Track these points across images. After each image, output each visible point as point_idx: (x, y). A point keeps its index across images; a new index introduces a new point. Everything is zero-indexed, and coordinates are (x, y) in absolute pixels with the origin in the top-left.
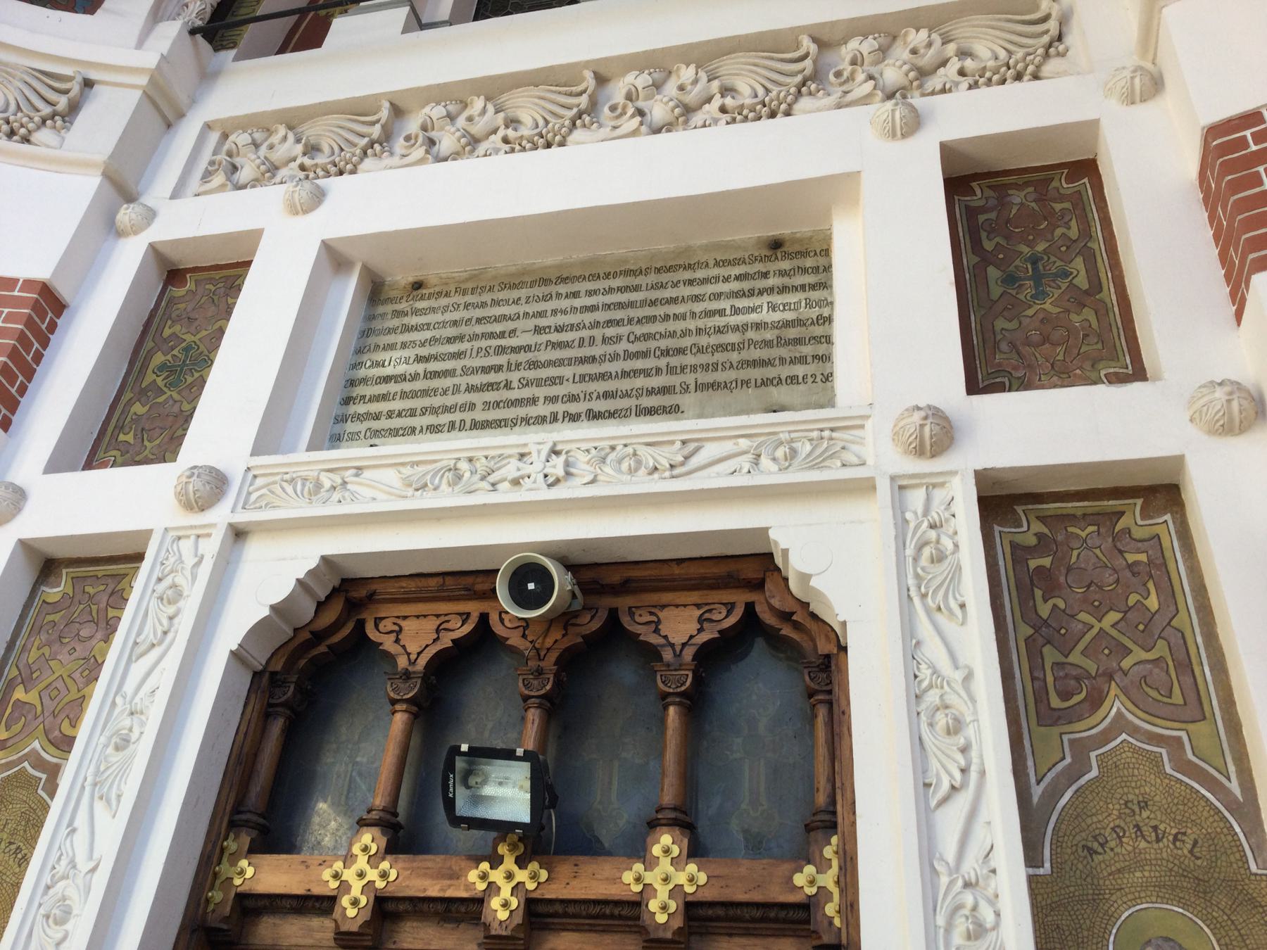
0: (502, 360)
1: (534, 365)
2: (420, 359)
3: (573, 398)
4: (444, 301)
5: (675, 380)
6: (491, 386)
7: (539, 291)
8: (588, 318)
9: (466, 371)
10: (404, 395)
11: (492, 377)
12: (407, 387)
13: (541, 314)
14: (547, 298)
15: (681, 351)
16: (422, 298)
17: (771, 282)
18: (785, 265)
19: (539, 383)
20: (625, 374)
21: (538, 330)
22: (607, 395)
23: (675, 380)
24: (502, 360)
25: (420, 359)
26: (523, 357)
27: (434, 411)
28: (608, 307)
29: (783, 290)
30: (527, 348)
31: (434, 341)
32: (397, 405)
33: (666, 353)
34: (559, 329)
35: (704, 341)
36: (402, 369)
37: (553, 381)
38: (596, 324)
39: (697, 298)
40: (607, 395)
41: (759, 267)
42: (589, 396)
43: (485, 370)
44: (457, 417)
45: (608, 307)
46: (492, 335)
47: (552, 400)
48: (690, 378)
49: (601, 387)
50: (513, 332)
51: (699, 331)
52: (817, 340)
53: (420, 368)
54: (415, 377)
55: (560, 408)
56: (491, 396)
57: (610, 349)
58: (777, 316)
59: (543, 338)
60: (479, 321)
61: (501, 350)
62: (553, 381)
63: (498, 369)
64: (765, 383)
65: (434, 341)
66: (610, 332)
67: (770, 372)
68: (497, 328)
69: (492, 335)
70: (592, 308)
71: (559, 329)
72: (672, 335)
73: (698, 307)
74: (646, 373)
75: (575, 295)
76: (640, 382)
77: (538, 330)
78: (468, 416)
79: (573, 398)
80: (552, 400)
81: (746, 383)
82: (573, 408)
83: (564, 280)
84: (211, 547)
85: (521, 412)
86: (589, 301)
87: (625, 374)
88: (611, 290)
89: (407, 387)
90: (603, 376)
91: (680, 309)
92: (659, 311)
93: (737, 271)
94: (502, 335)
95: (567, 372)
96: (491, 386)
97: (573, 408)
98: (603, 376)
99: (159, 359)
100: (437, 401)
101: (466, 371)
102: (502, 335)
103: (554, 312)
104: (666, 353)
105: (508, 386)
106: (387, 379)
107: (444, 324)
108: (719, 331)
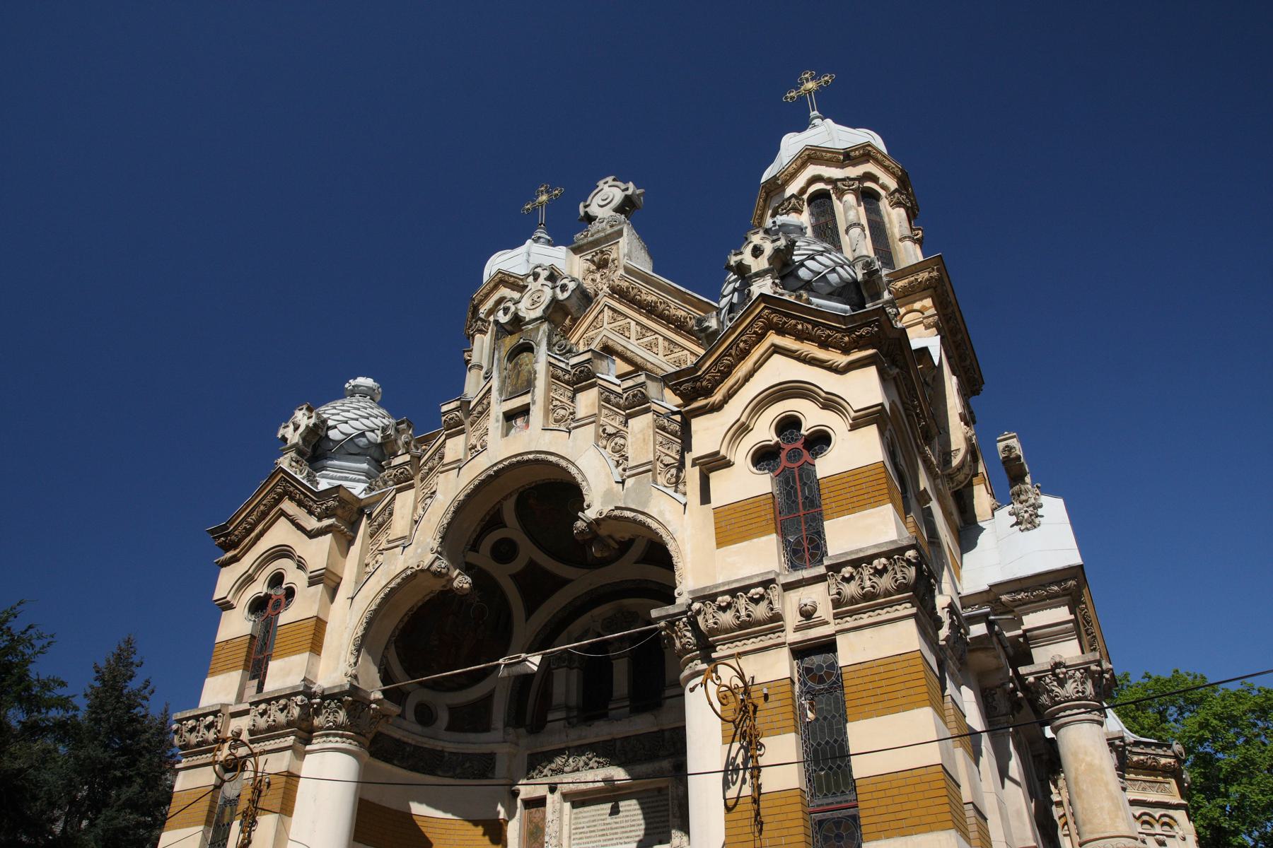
0: (605, 827)
1: (612, 829)
3: (621, 838)
6: (603, 835)
9: (598, 831)
11: (604, 832)
19: (613, 834)
20: (631, 831)
22: (628, 837)
24: (605, 827)
26: (609, 826)
30: (609, 824)
31: (589, 821)
32: (585, 840)
37: (616, 833)
40: (628, 837)
47: (616, 839)
55: (618, 841)
56: (604, 838)
57: (627, 824)
61: (604, 824)
62: (616, 833)
63: (604, 830)
66: (627, 819)
69: (602, 820)
78: (600, 843)
79: (621, 838)
80: (616, 839)
81: (654, 833)
82: (621, 841)
90: (626, 832)
96: (603, 835)
97: (621, 841)
98: (626, 832)
100: (593, 839)
101: (598, 831)
107: (591, 816)
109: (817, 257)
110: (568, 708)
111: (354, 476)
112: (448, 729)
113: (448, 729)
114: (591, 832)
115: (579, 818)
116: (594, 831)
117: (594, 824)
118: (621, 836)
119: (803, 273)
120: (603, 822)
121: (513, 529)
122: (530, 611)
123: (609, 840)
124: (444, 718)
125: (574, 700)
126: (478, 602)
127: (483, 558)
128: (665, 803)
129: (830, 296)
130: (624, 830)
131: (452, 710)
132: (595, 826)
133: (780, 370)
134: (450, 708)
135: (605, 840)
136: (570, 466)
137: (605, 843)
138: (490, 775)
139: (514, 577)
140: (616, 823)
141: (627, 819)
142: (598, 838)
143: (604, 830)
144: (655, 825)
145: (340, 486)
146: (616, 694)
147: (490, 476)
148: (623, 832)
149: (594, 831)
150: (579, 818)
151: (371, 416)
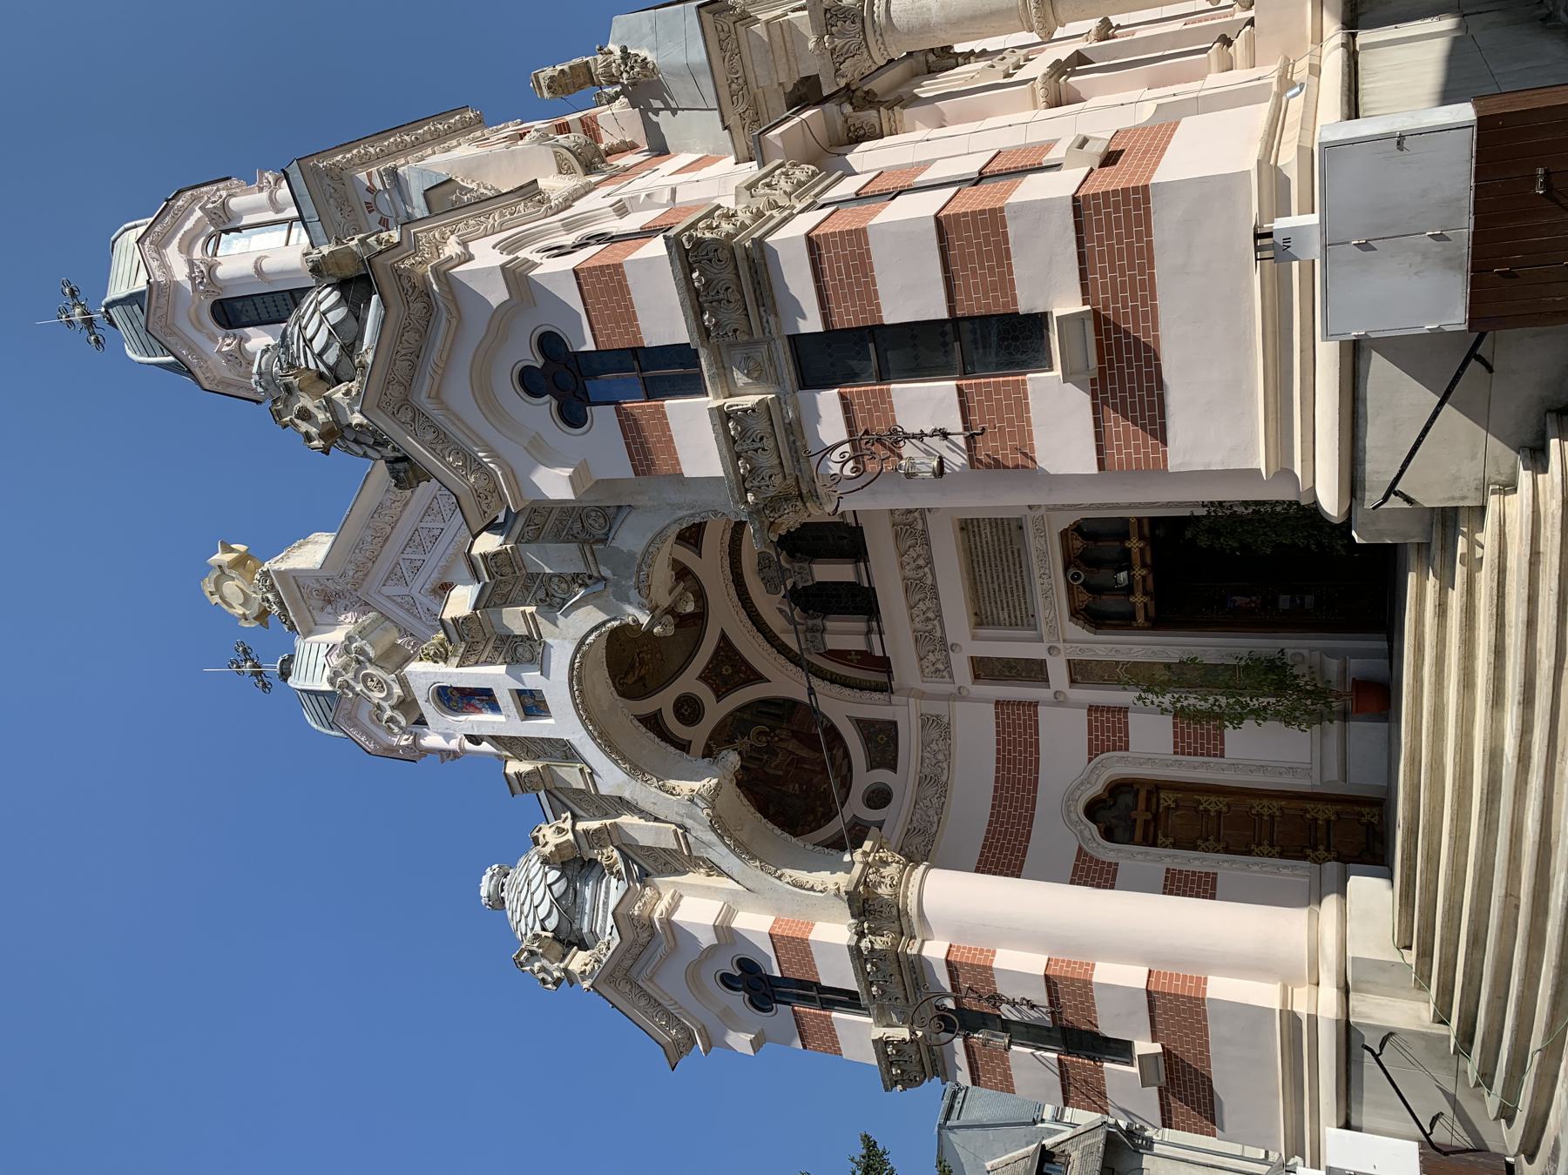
0: (1003, 591)
1: (1005, 582)
2: (1003, 609)
3: (1015, 572)
6: (1012, 592)
7: (979, 584)
8: (988, 571)
17: (976, 529)
18: (970, 527)
20: (1007, 561)
21: (993, 582)
22: (1014, 565)
24: (1003, 591)
25: (1003, 609)
29: (979, 526)
30: (999, 585)
32: (1018, 613)
33: (1000, 552)
36: (1006, 614)
37: (1010, 577)
39: (982, 547)
40: (1014, 565)
41: (971, 533)
48: (1009, 547)
49: (1012, 566)
52: (996, 523)
53: (1006, 609)
56: (1015, 591)
58: (988, 528)
61: (1000, 591)
62: (1010, 577)
63: (1006, 592)
64: (1010, 530)
66: (993, 565)
67: (1006, 529)
68: (992, 593)
73: (985, 546)
77: (993, 582)
79: (1015, 572)
83: (975, 579)
84: (1068, 645)
85: (1020, 585)
86: (983, 571)
87: (1007, 561)
90: (1008, 566)
92: (986, 555)
93: (972, 538)
96: (1012, 592)
98: (1008, 566)
99: (1007, 674)
100: (1017, 604)
104: (1000, 552)
106: (1010, 617)
108: (993, 541)
109: (308, 336)
110: (869, 632)
111: (603, 894)
112: (894, 769)
113: (894, 769)
114: (1008, 606)
116: (1007, 602)
119: (331, 357)
121: (664, 701)
122: (758, 678)
123: (1017, 586)
124: (882, 776)
125: (861, 626)
126: (749, 739)
127: (698, 734)
128: (975, 522)
129: (360, 321)
130: (1006, 568)
131: (872, 766)
132: (1001, 601)
133: (459, 393)
134: (872, 768)
135: (1018, 589)
136: (587, 642)
137: (1021, 590)
138: (946, 720)
139: (719, 697)
140: (998, 576)
141: (993, 565)
143: (1006, 592)
145: (613, 914)
146: (852, 578)
147: (601, 735)
148: (1009, 571)
149: (1007, 602)
151: (527, 877)
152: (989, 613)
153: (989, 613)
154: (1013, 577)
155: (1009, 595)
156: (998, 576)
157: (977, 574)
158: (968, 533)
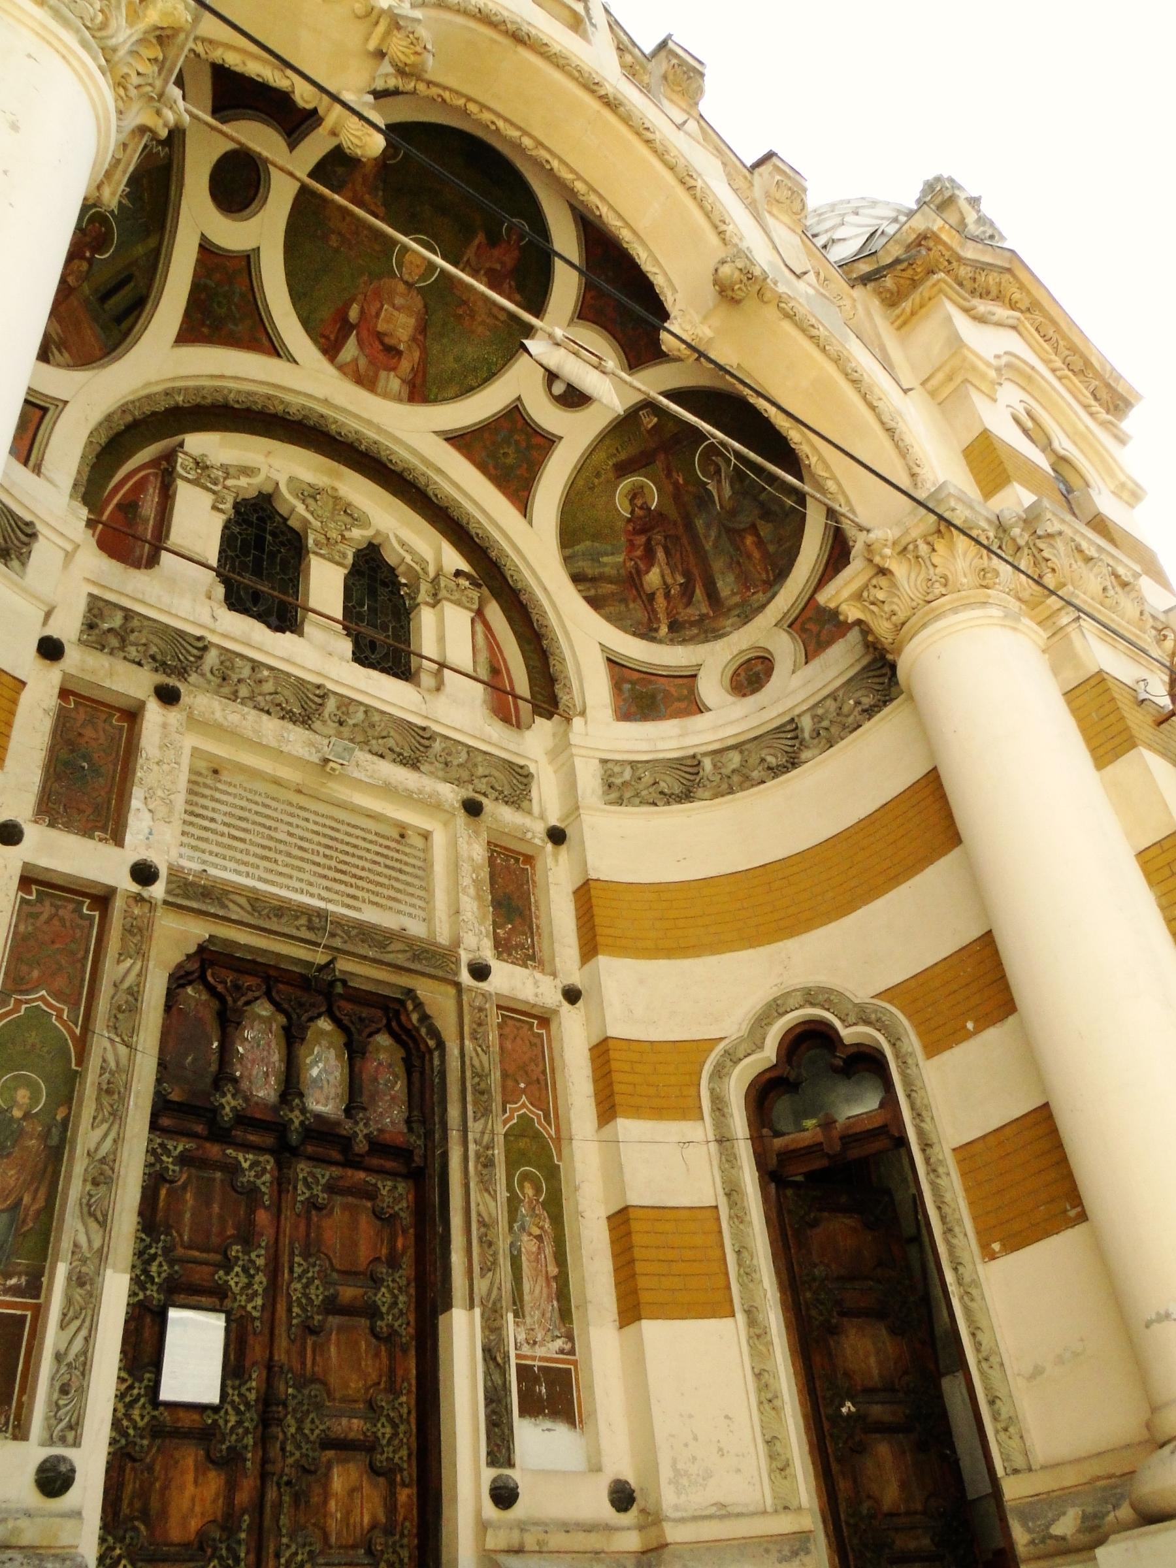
0: (272, 844)
1: (289, 855)
3: (311, 884)
4: (231, 790)
5: (359, 894)
8: (316, 838)
9: (252, 843)
10: (218, 844)
12: (220, 839)
13: (290, 824)
14: (292, 815)
15: (361, 878)
16: (220, 781)
19: (293, 867)
20: (335, 880)
21: (290, 834)
22: (327, 888)
23: (359, 894)
24: (272, 844)
26: (281, 847)
27: (238, 861)
28: (325, 835)
31: (231, 815)
32: (216, 849)
33: (354, 876)
34: (301, 838)
35: (372, 877)
37: (300, 869)
38: (319, 844)
40: (327, 888)
41: (393, 845)
42: (318, 886)
43: (264, 847)
44: (251, 870)
45: (325, 835)
46: (264, 826)
48: (366, 895)
50: (276, 829)
51: (370, 870)
54: (222, 835)
57: (328, 862)
59: (294, 840)
60: (257, 813)
61: (271, 838)
63: (270, 849)
64: (399, 912)
65: (231, 815)
66: (328, 852)
68: (268, 823)
69: (264, 826)
70: (317, 833)
71: (301, 838)
72: (357, 867)
74: (346, 884)
75: (307, 820)
76: (342, 888)
77: (290, 834)
81: (391, 908)
86: (316, 828)
88: (324, 826)
89: (220, 839)
91: (357, 852)
94: (270, 828)
95: (307, 866)
100: (239, 856)
101: (252, 843)
102: (270, 828)
103: (297, 826)
104: (354, 876)
105: (276, 861)
107: (235, 806)
115: (204, 796)
116: (243, 840)
117: (244, 825)
118: (313, 879)
120: (267, 832)
139: (207, 249)
140: (301, 848)
141: (328, 852)
142: (252, 860)
144: (392, 893)
149: (243, 840)
150: (204, 796)
152: (218, 795)
153: (218, 795)
154: (301, 875)
155: (259, 851)
156: (301, 848)
157: (312, 817)
158: (394, 840)
